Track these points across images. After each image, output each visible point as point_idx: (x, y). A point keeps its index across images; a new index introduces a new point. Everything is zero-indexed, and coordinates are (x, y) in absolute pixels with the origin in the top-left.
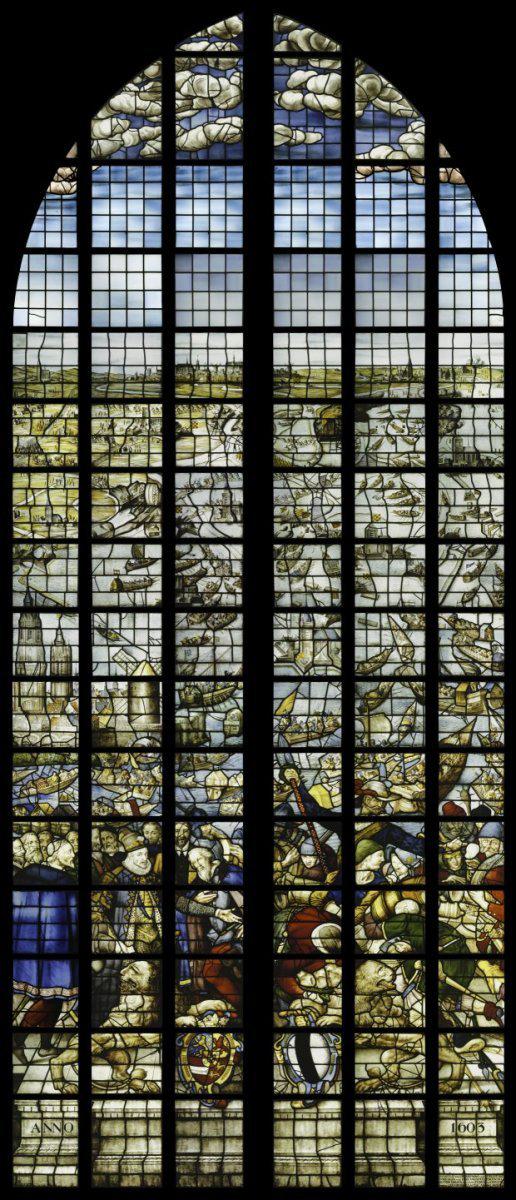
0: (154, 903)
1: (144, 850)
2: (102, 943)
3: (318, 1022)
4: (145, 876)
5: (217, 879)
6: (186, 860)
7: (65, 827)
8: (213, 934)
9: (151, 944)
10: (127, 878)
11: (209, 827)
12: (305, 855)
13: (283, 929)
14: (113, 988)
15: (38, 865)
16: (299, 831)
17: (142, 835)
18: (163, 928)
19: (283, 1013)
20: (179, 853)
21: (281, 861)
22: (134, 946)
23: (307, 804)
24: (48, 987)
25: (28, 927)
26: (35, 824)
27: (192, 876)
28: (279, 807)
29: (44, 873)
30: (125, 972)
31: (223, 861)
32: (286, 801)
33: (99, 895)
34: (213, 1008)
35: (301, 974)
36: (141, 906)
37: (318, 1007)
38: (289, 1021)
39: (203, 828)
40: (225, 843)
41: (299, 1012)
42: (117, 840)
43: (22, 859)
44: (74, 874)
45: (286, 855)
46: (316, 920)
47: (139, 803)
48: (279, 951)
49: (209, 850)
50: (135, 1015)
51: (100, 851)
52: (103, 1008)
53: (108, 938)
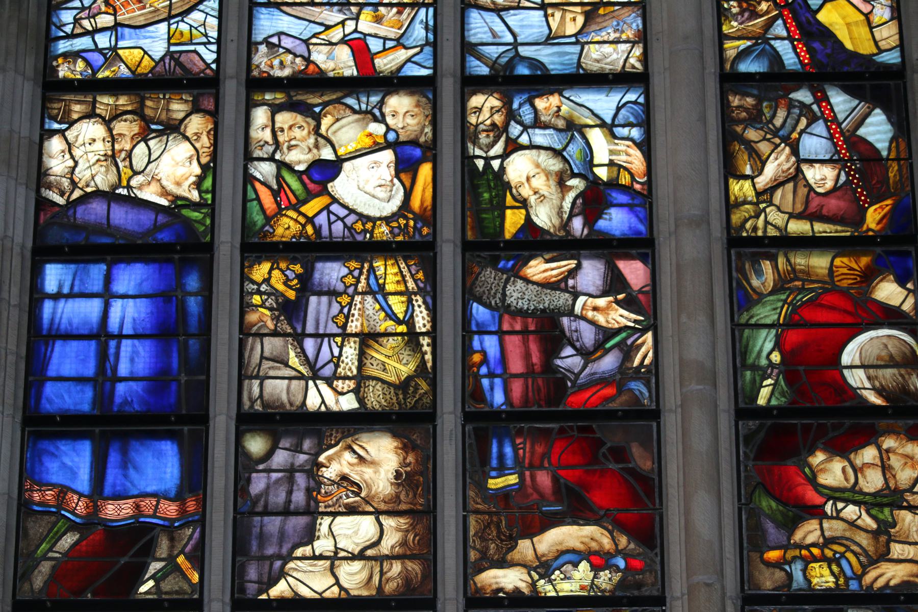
0: (411, 285)
1: (388, 156)
2: (268, 383)
3: (868, 579)
4: (387, 220)
5: (577, 224)
6: (499, 182)
7: (178, 108)
8: (569, 360)
9: (404, 386)
10: (338, 227)
11: (554, 100)
12: (811, 162)
13: (769, 346)
14: (299, 497)
15: (109, 196)
16: (791, 105)
17: (382, 120)
18: (434, 345)
19: (773, 555)
20: (480, 164)
21: (752, 178)
22: (356, 391)
23: (817, 45)
24: (118, 496)
25: (74, 345)
26: (106, 100)
27: (513, 221)
28: (742, 55)
29: (120, 216)
30: (330, 459)
31: (594, 183)
32: (762, 39)
33: (266, 267)
34: (578, 546)
35: (818, 458)
36: (379, 291)
37: (863, 540)
38: (790, 576)
39: (540, 104)
40: (596, 137)
41: (815, 551)
42: (317, 131)
43: (66, 183)
44: (195, 215)
45: (764, 163)
46: (849, 320)
47: (375, 45)
48: (761, 401)
49: (557, 153)
50: (357, 565)
51: (271, 159)
52: (270, 551)
53: (293, 373)
